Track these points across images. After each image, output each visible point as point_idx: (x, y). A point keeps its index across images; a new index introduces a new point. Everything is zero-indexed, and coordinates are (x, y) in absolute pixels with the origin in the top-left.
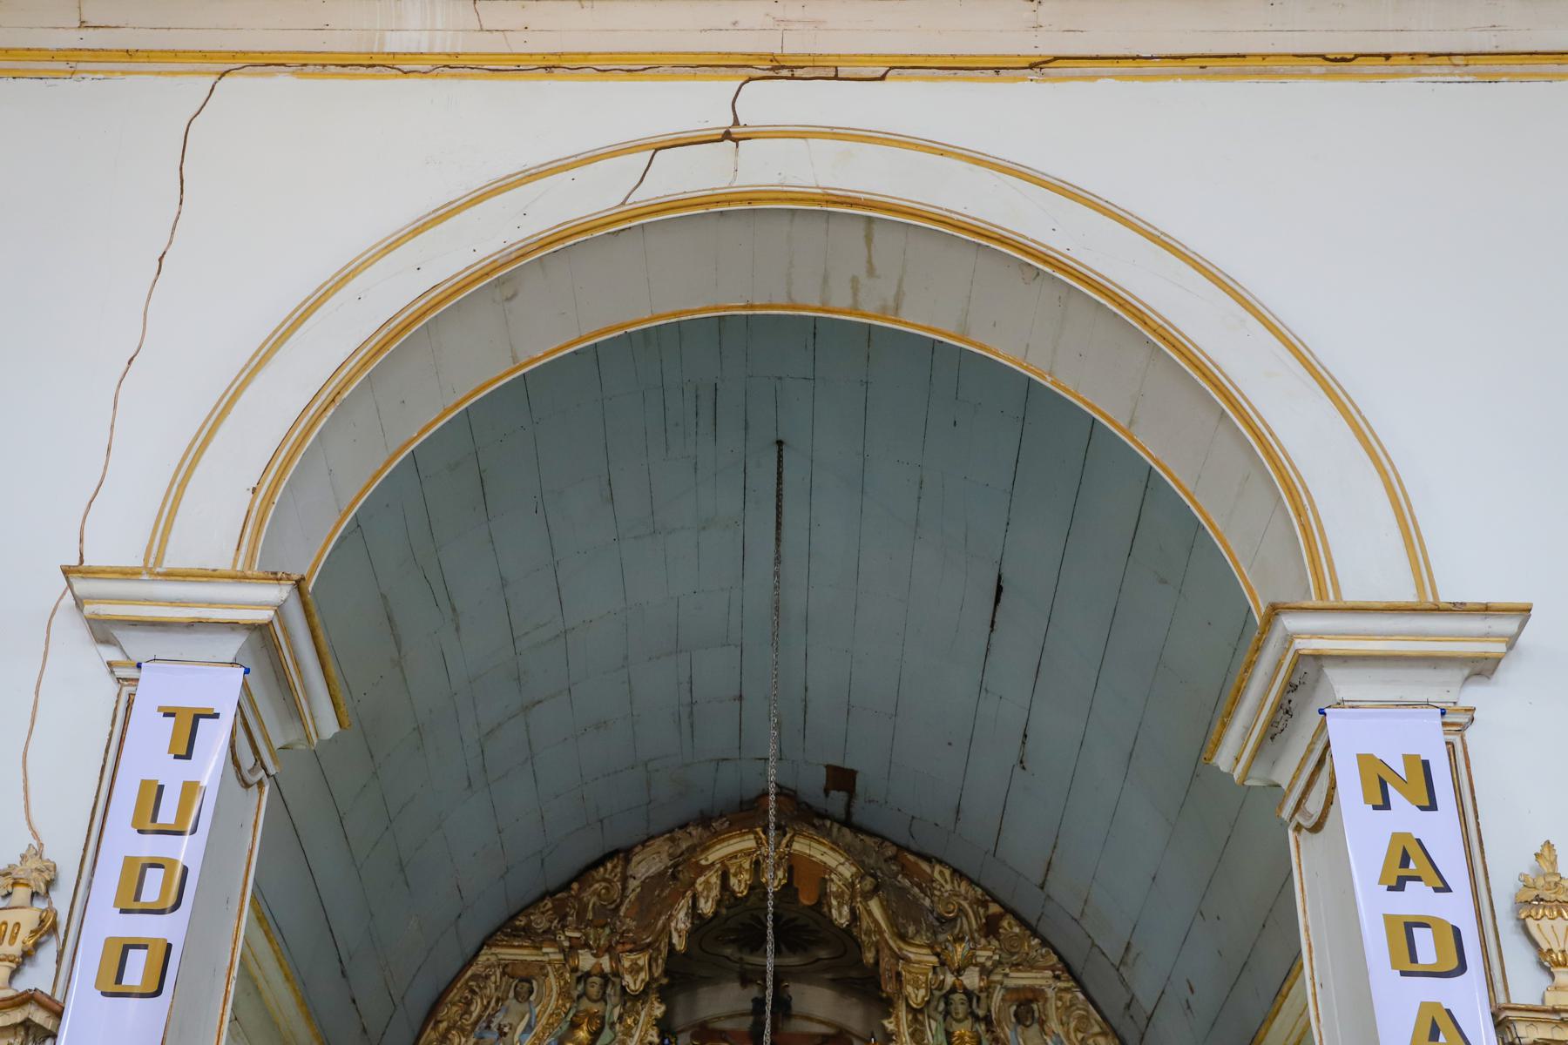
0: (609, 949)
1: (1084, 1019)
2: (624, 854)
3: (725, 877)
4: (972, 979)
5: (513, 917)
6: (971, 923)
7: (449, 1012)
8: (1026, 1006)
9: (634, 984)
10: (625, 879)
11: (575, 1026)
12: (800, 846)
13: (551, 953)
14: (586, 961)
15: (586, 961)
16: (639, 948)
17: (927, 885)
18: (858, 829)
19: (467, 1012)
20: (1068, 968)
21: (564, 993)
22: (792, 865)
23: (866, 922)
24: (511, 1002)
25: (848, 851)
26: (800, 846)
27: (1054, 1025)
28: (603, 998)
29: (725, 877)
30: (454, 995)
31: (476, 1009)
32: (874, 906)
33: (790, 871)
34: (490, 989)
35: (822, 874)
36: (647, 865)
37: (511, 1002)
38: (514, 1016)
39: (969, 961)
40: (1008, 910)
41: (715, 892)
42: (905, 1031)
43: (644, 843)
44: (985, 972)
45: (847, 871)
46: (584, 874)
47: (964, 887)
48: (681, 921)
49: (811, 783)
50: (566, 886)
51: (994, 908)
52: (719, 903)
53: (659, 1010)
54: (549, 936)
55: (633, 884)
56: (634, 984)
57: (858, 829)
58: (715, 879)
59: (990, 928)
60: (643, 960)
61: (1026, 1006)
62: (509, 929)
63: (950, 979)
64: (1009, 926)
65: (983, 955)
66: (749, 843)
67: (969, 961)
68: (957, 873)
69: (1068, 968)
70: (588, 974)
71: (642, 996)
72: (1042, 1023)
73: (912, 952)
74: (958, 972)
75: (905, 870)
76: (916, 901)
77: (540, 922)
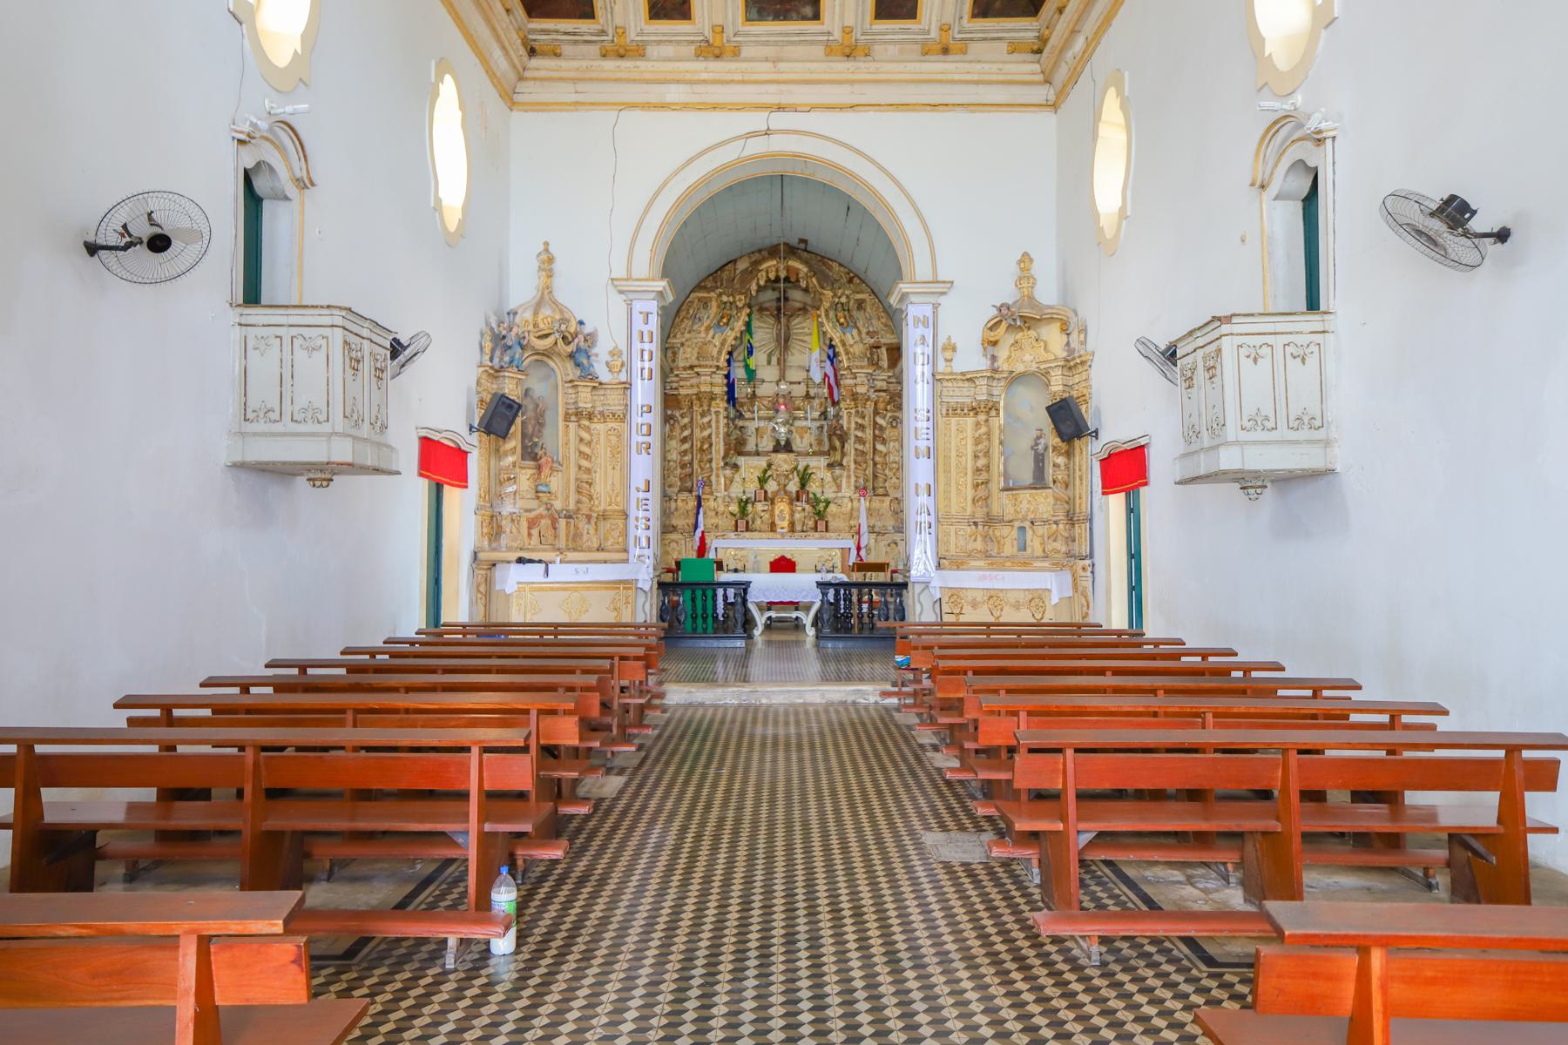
0: (732, 295)
1: (878, 308)
2: (734, 261)
3: (767, 272)
4: (843, 300)
5: (700, 282)
6: (844, 280)
7: (683, 314)
8: (860, 305)
9: (740, 304)
10: (735, 270)
11: (722, 317)
12: (791, 263)
13: (712, 294)
14: (725, 298)
15: (725, 298)
16: (742, 294)
17: (830, 268)
18: (809, 252)
19: (688, 313)
20: (873, 293)
21: (718, 307)
22: (788, 269)
23: (811, 285)
24: (702, 309)
25: (806, 263)
26: (791, 263)
27: (868, 310)
28: (731, 309)
29: (767, 272)
30: (684, 307)
31: (691, 311)
32: (814, 280)
33: (788, 271)
34: (695, 305)
35: (797, 272)
36: (742, 265)
37: (702, 309)
38: (703, 314)
39: (843, 294)
40: (856, 275)
41: (765, 278)
42: (823, 314)
43: (741, 257)
44: (847, 297)
45: (805, 270)
46: (722, 268)
47: (842, 269)
48: (754, 287)
49: (794, 242)
50: (716, 272)
51: (852, 275)
52: (766, 282)
53: (748, 311)
54: (713, 289)
55: (738, 272)
56: (740, 304)
57: (809, 252)
58: (764, 274)
59: (850, 281)
60: (743, 297)
61: (860, 305)
62: (699, 287)
63: (837, 300)
64: (856, 280)
65: (847, 292)
66: (775, 262)
67: (843, 294)
68: (841, 265)
69: (873, 293)
70: (725, 303)
71: (743, 307)
72: (865, 310)
73: (825, 292)
74: (840, 298)
75: (824, 264)
76: (828, 276)
77: (709, 285)
